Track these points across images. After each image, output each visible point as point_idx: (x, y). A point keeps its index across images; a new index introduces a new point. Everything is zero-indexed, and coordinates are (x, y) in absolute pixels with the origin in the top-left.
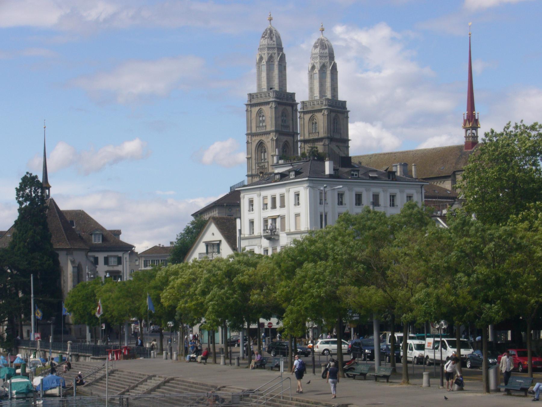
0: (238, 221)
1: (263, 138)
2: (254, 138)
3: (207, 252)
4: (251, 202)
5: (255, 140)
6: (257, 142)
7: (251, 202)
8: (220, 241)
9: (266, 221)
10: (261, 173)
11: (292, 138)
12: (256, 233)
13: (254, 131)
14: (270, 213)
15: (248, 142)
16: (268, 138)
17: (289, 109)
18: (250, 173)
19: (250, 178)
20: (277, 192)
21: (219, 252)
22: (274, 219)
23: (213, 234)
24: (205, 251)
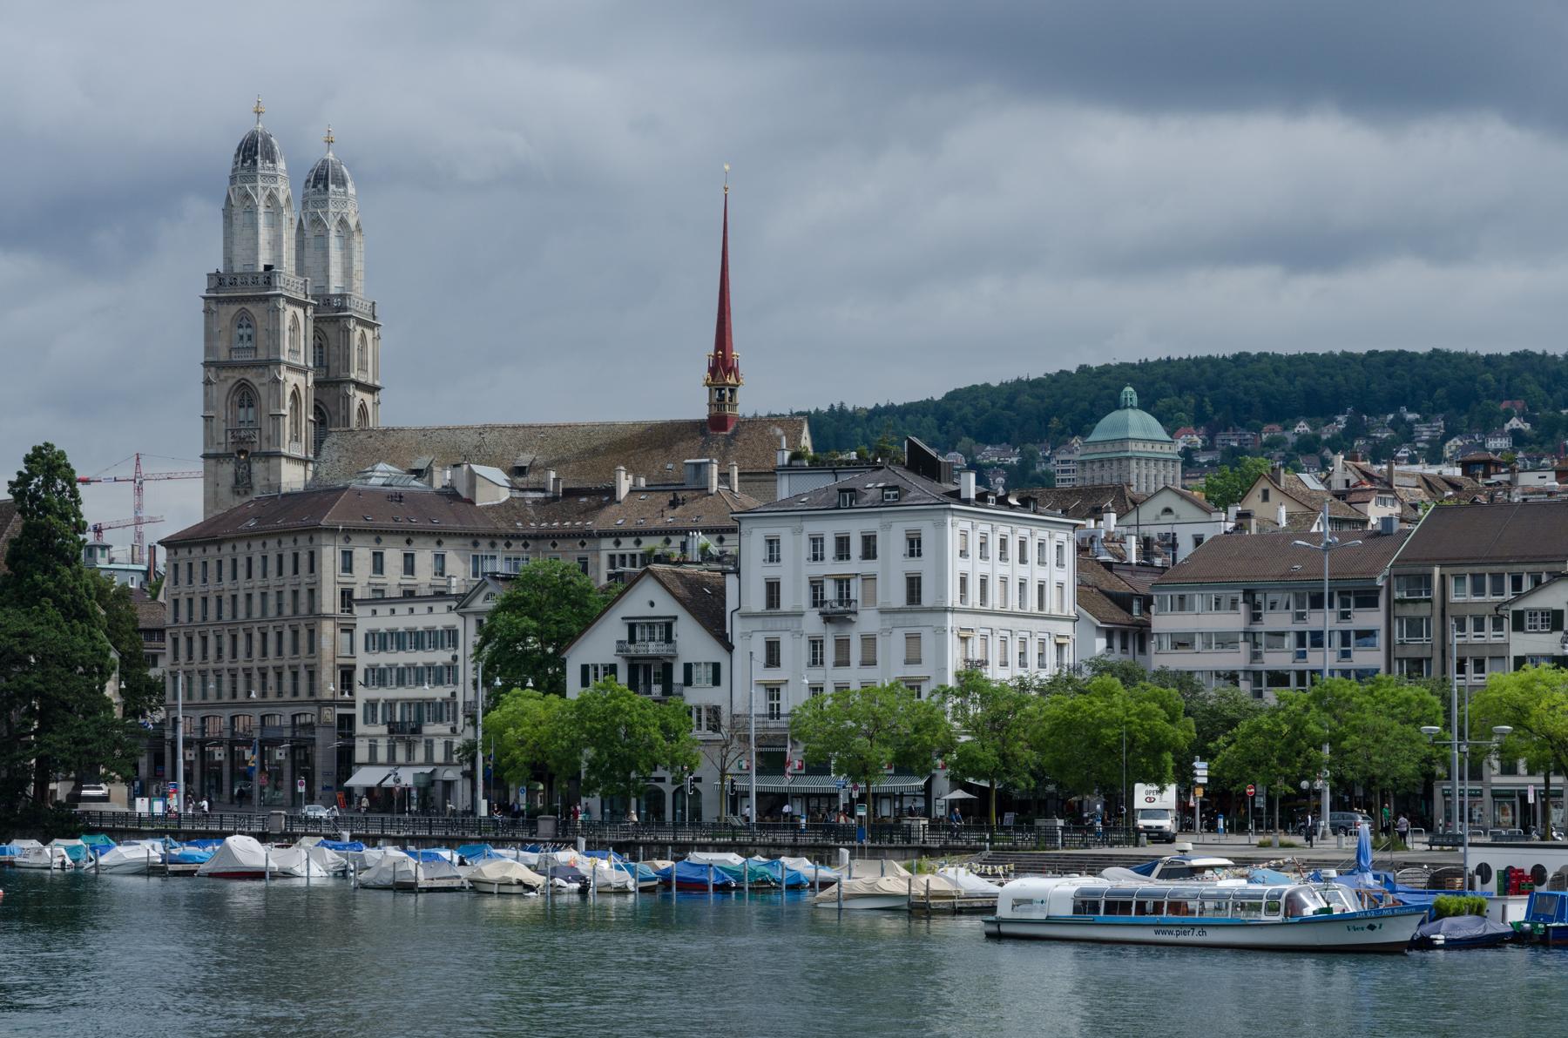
0: (731, 581)
1: (250, 375)
2: (223, 374)
3: (632, 639)
4: (773, 544)
5: (226, 379)
6: (231, 382)
7: (773, 544)
8: (676, 618)
9: (816, 585)
10: (240, 452)
11: (302, 378)
12: (786, 604)
13: (223, 356)
14: (831, 566)
15: (207, 382)
16: (262, 375)
17: (300, 312)
18: (212, 451)
19: (212, 462)
20: (855, 528)
21: (668, 639)
22: (843, 582)
23: (652, 604)
24: (625, 637)
